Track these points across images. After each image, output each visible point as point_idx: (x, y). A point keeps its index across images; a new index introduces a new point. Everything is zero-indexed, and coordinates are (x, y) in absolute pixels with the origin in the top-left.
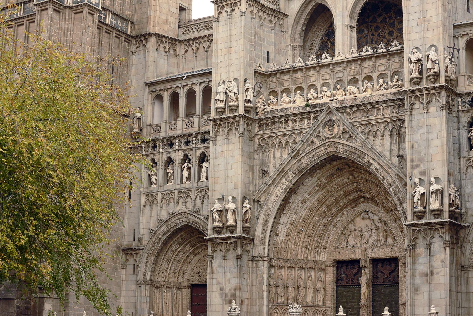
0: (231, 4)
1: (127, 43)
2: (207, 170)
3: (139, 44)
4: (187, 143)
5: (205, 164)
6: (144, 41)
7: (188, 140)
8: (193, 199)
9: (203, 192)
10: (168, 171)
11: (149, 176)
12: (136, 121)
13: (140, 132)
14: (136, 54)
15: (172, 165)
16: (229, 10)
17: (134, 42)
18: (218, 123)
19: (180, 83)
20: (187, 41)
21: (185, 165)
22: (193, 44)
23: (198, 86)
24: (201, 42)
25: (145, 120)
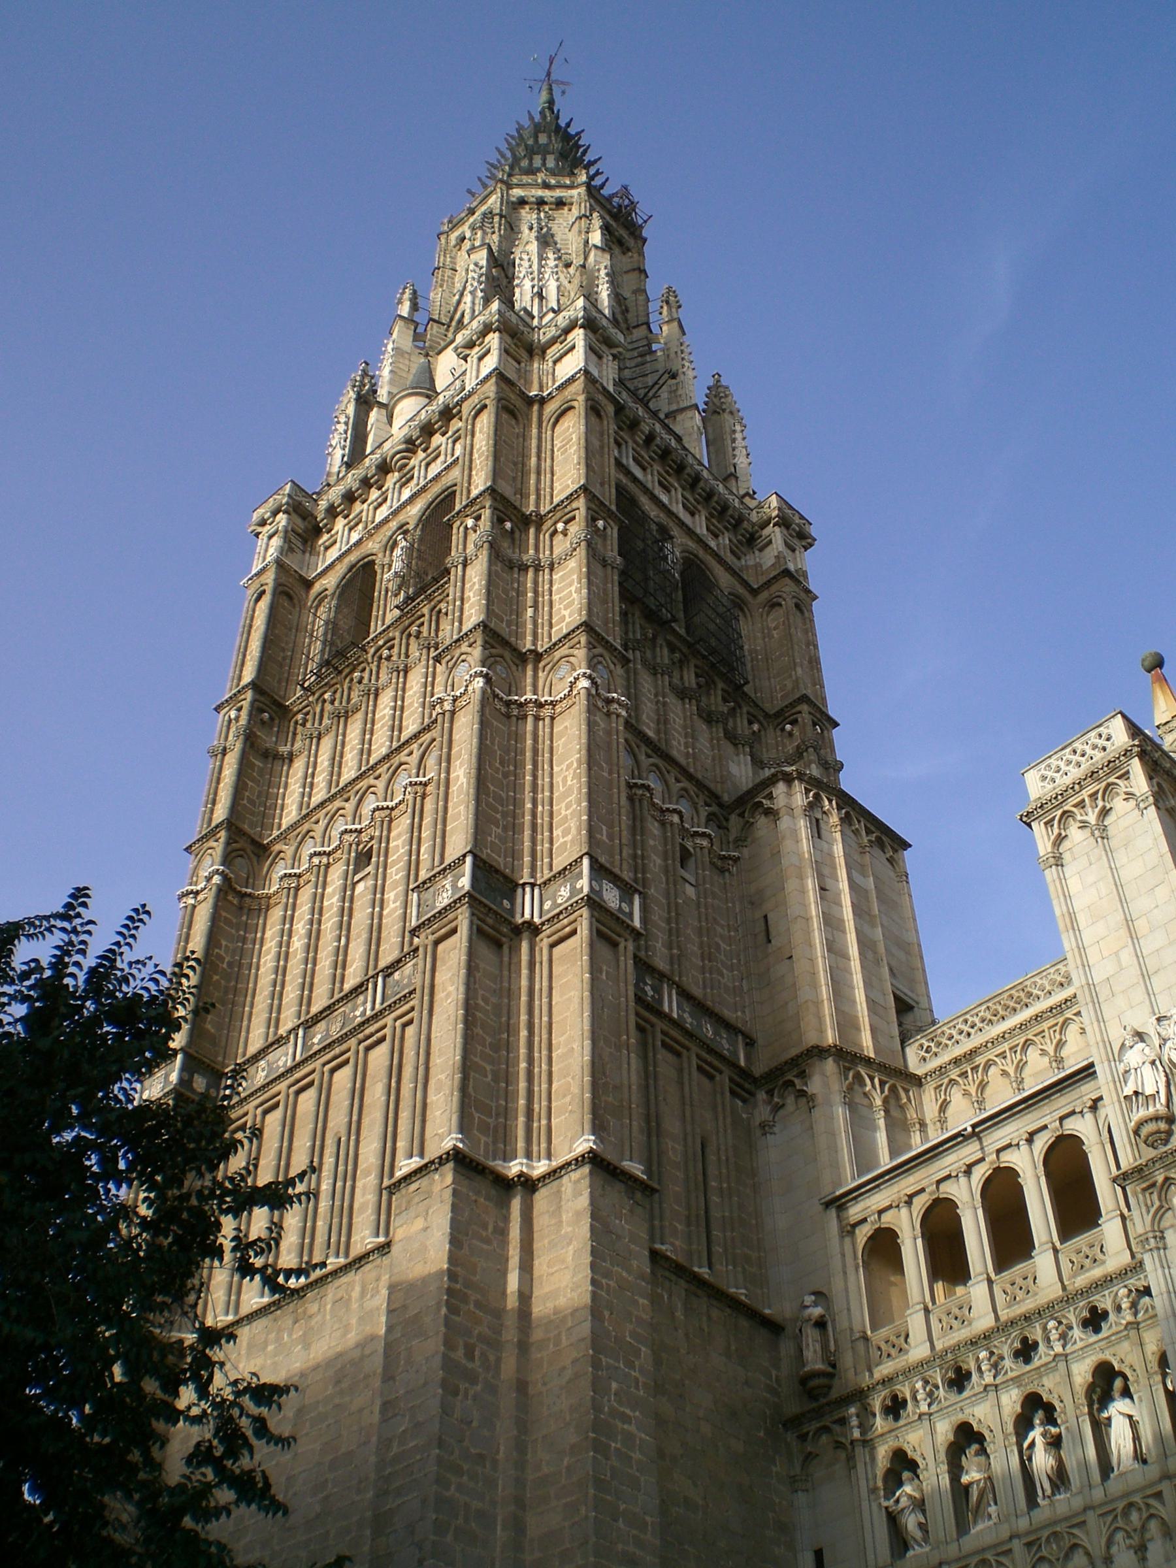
0: (1093, 796)
1: (740, 1103)
2: (1134, 1424)
3: (782, 1096)
4: (1026, 1351)
5: (1118, 1409)
6: (797, 1081)
7: (1025, 1340)
8: (1098, 1551)
9: (1134, 1516)
10: (965, 1479)
11: (893, 1519)
12: (811, 1336)
13: (830, 1370)
14: (776, 1129)
15: (983, 1451)
16: (1092, 818)
17: (762, 1095)
18: (1160, 1179)
19: (952, 1161)
20: (941, 1070)
21: (1036, 1434)
22: (964, 1075)
23: (1024, 1147)
24: (988, 1065)
25: (842, 1323)
